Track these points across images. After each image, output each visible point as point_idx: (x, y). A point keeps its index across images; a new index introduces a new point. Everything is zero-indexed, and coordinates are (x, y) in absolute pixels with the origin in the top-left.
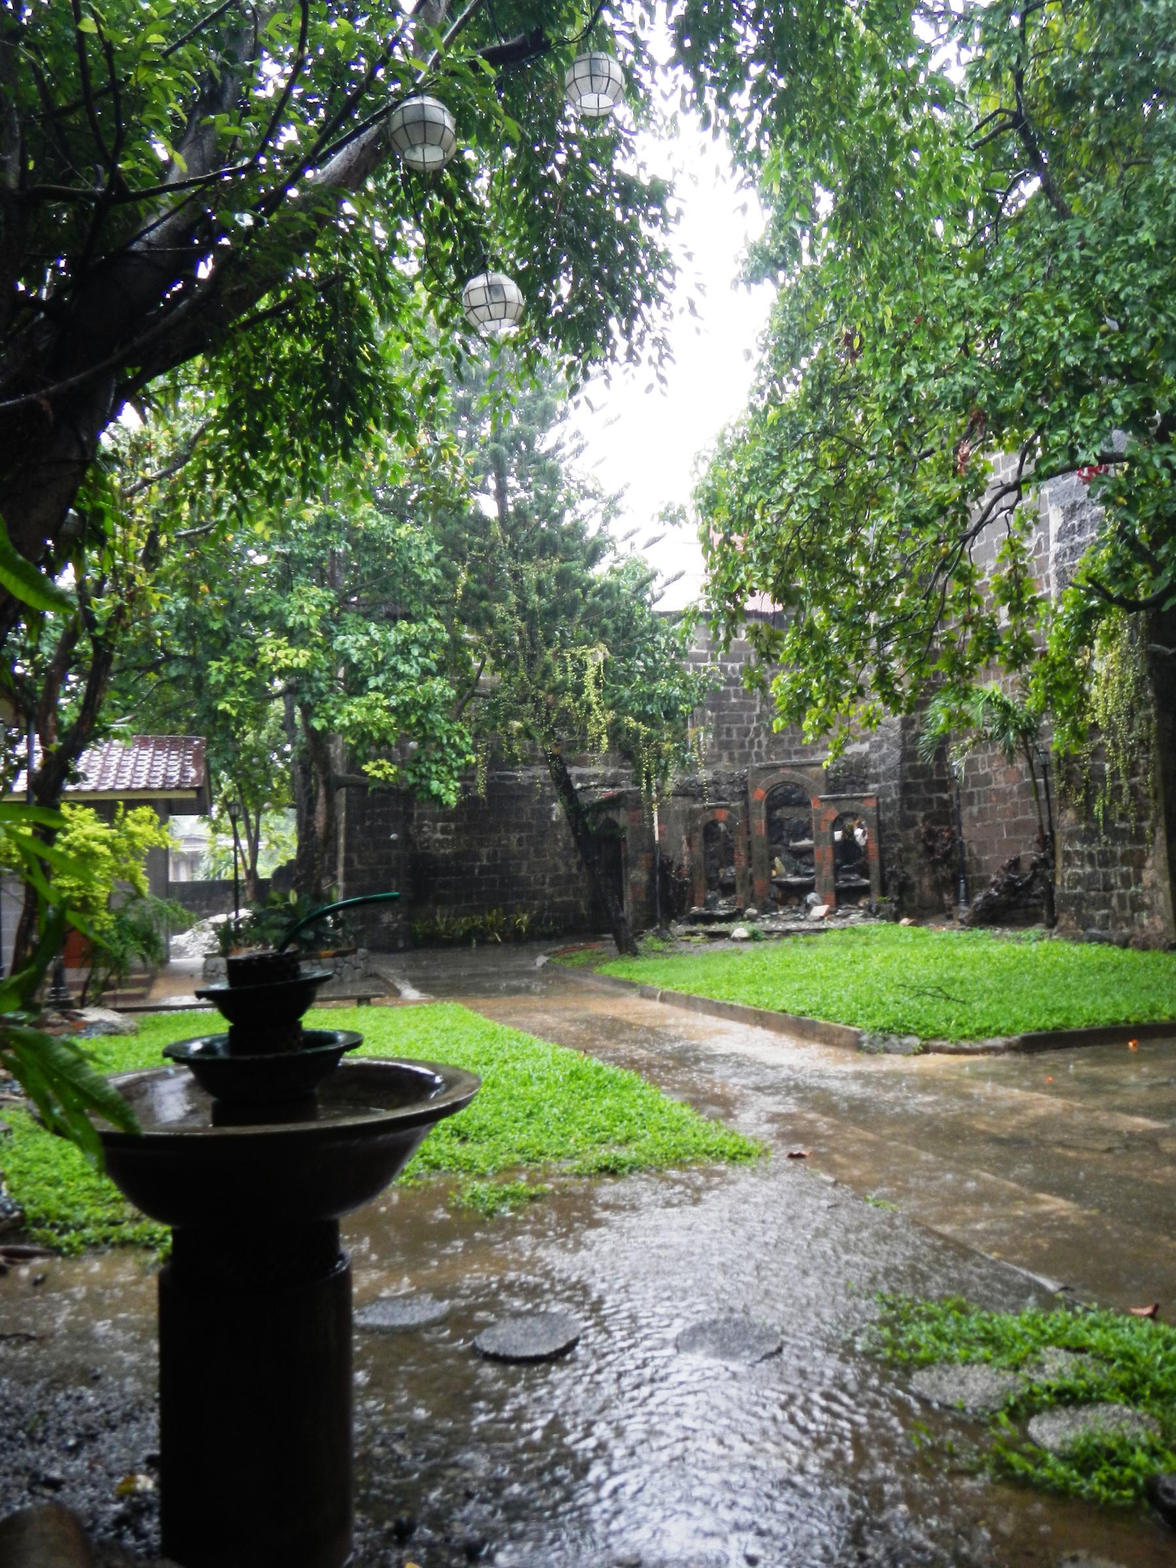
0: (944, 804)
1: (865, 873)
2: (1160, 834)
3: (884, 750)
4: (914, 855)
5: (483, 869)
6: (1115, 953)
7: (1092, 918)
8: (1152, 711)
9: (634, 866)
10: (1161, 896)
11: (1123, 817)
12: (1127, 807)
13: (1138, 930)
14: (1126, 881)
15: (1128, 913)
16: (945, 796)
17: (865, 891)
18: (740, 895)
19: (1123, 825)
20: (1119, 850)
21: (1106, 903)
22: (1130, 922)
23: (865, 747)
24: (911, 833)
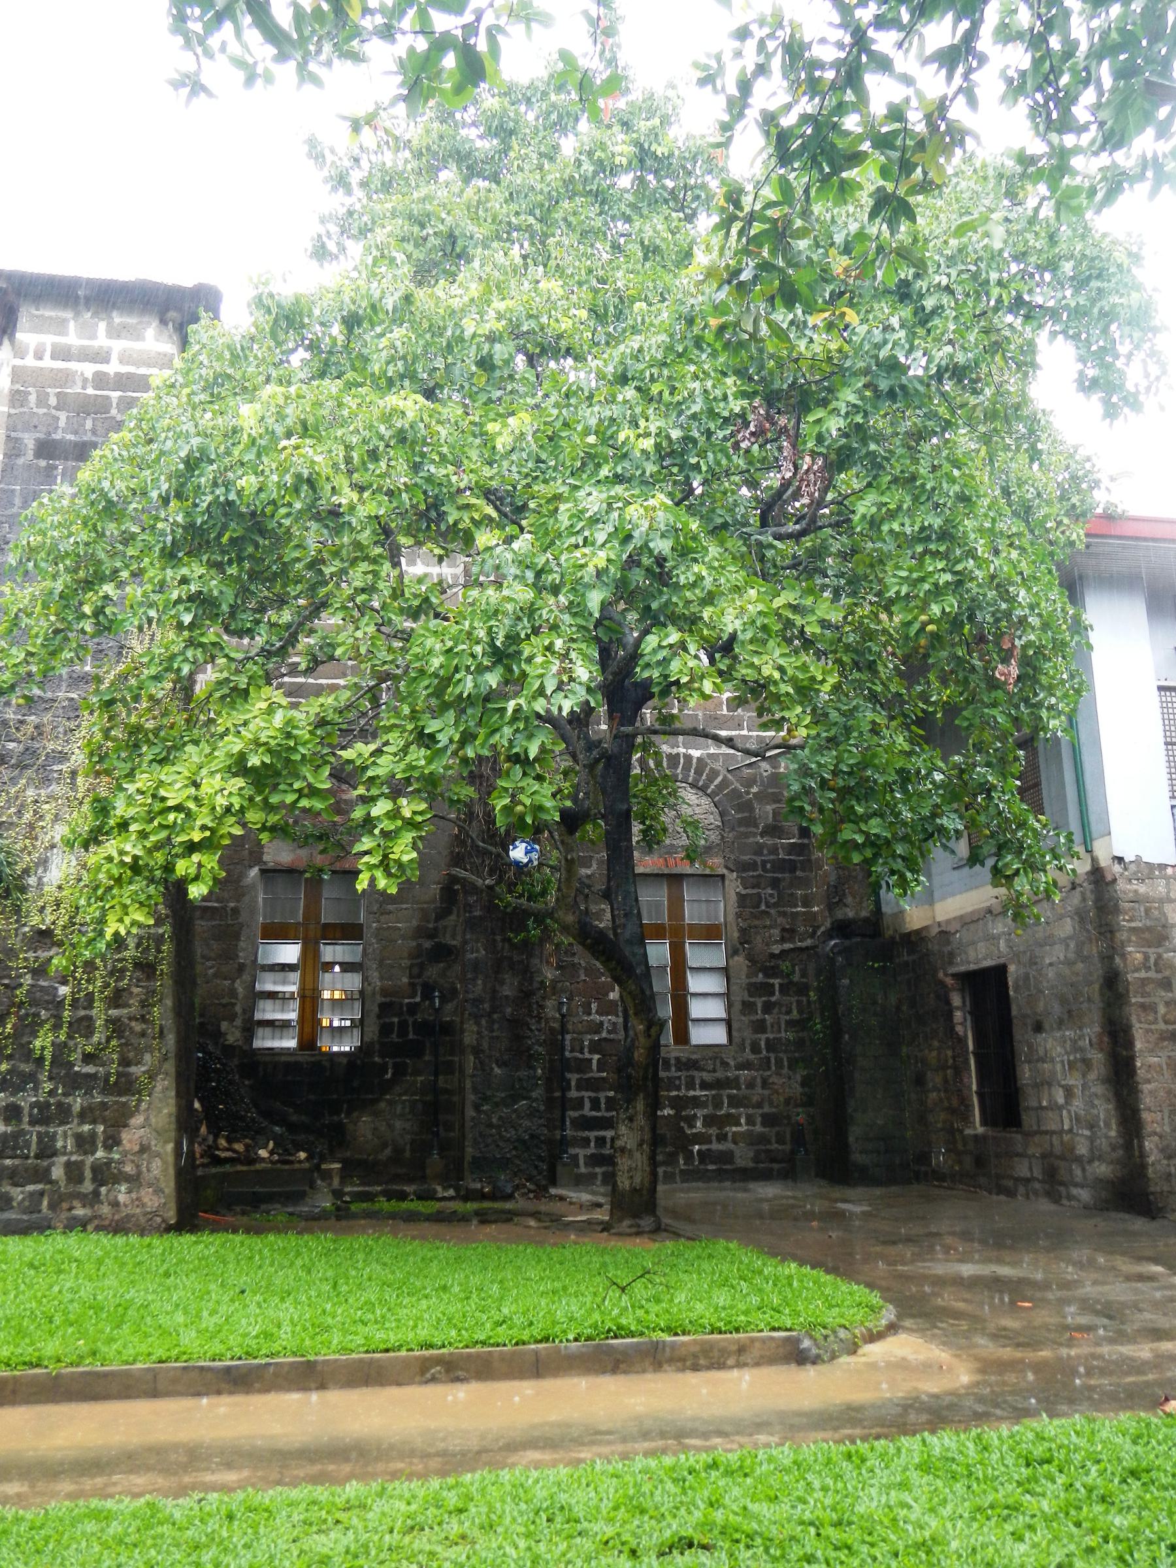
11: (88, 1058)
12: (101, 1048)
13: (105, 1209)
14: (85, 1143)
15: (88, 1186)
19: (90, 1069)
20: (77, 1103)
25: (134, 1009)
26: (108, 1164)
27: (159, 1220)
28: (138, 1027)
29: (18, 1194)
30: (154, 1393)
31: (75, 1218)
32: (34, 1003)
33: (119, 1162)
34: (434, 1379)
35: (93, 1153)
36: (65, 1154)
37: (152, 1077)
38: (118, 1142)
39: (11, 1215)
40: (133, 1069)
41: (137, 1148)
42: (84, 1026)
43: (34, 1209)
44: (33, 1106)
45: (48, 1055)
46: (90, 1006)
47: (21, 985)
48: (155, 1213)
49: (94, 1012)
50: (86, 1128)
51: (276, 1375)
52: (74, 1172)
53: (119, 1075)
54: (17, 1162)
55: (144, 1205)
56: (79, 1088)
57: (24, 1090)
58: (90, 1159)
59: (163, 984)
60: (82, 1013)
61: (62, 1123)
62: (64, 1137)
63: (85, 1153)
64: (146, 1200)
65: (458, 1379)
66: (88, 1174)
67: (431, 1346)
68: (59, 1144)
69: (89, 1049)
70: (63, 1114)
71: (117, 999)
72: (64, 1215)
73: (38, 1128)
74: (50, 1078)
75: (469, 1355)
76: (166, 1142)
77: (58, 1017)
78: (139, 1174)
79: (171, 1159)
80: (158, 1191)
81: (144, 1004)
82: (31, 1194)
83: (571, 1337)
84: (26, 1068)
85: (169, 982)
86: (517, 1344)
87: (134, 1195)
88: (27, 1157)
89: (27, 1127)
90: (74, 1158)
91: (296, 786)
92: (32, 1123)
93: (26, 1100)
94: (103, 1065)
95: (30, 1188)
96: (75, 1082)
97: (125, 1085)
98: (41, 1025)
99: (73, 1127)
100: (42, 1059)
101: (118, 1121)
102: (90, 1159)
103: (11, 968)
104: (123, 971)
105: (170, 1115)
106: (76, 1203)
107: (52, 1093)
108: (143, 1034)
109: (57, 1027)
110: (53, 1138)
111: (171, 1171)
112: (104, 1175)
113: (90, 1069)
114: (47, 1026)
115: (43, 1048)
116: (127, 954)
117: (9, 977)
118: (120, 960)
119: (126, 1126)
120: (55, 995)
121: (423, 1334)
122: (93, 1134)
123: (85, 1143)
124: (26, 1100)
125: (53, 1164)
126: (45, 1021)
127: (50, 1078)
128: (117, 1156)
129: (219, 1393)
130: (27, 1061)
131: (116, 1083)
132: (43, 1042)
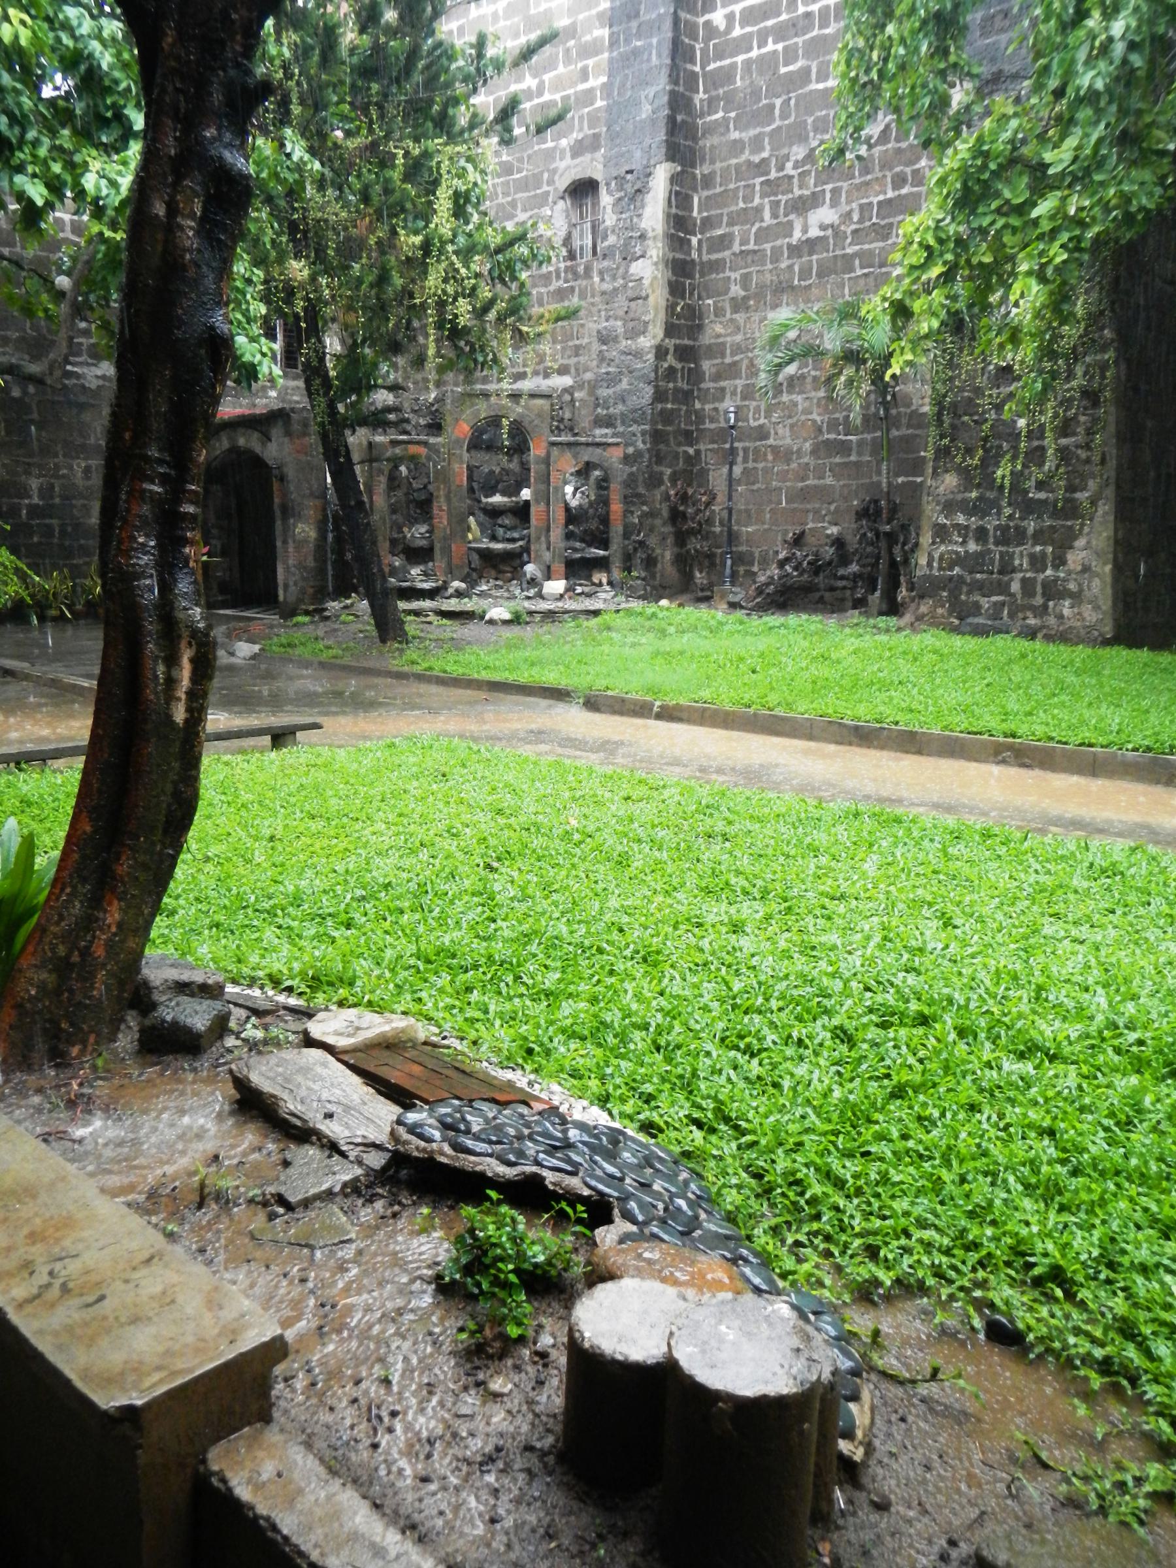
0: (689, 460)
1: (605, 545)
2: (1105, 509)
3: (624, 384)
4: (658, 522)
5: (33, 510)
6: (1024, 644)
7: (977, 606)
8: (1109, 355)
9: (299, 516)
10: (1096, 582)
11: (1040, 486)
12: (1051, 476)
13: (1052, 621)
14: (1037, 563)
15: (1038, 600)
16: (691, 451)
17: (602, 564)
18: (439, 563)
19: (1042, 495)
20: (1031, 526)
21: (1003, 589)
22: (1043, 611)
23: (567, 381)
24: (658, 494)
25: (1080, 439)
26: (1057, 579)
27: (1096, 633)
28: (1083, 454)
29: (985, 603)
30: (811, 737)
31: (1028, 626)
32: (998, 436)
33: (1064, 580)
34: (1003, 762)
35: (1044, 571)
36: (1021, 571)
37: (1093, 502)
38: (1063, 562)
39: (980, 620)
40: (1078, 495)
41: (1079, 568)
42: (1036, 455)
43: (997, 616)
44: (996, 528)
45: (1007, 482)
46: (1042, 437)
47: (986, 420)
48: (1091, 628)
49: (1046, 442)
50: (1038, 548)
51: (889, 738)
52: (1028, 586)
53: (1067, 500)
54: (984, 576)
55: (1084, 619)
56: (1032, 513)
57: (989, 514)
58: (1042, 576)
59: (1108, 412)
60: (1036, 443)
61: (1020, 544)
62: (1020, 556)
63: (1037, 572)
64: (1086, 615)
65: (1024, 766)
66: (1039, 589)
67: (1014, 736)
68: (1017, 562)
69: (1040, 476)
70: (1020, 536)
71: (1065, 428)
72: (1020, 623)
73: (1001, 548)
74: (1010, 504)
75: (1036, 747)
76: (1105, 564)
77: (1015, 448)
78: (1081, 591)
79: (1109, 579)
80: (1097, 608)
81: (1090, 432)
82: (995, 604)
83: (1130, 746)
84: (991, 495)
85: (1112, 409)
86: (1080, 745)
87: (1076, 610)
88: (992, 573)
89: (992, 547)
90: (1028, 575)
91: (993, 206)
92: (997, 544)
93: (991, 523)
94: (1052, 491)
95: (994, 599)
96: (1029, 508)
97: (1071, 510)
98: (1003, 456)
99: (1026, 548)
100: (1002, 487)
101: (1064, 544)
102: (1042, 576)
103: (979, 405)
104: (1072, 399)
105: (1108, 538)
106: (1029, 614)
107: (1011, 517)
108: (1088, 461)
109: (1014, 458)
110: (1012, 556)
111: (1109, 591)
112: (1053, 591)
113: (1042, 495)
114: (1008, 457)
115: (1003, 477)
116: (1074, 383)
117: (977, 413)
118: (1068, 390)
119: (1071, 547)
120: (1014, 428)
121: (1011, 726)
122: (1043, 553)
123: (1037, 563)
124: (991, 523)
125: (1012, 580)
126: (1006, 452)
127: (1010, 504)
128: (1062, 575)
129: (850, 744)
130: (992, 489)
131: (1063, 508)
132: (1002, 472)
